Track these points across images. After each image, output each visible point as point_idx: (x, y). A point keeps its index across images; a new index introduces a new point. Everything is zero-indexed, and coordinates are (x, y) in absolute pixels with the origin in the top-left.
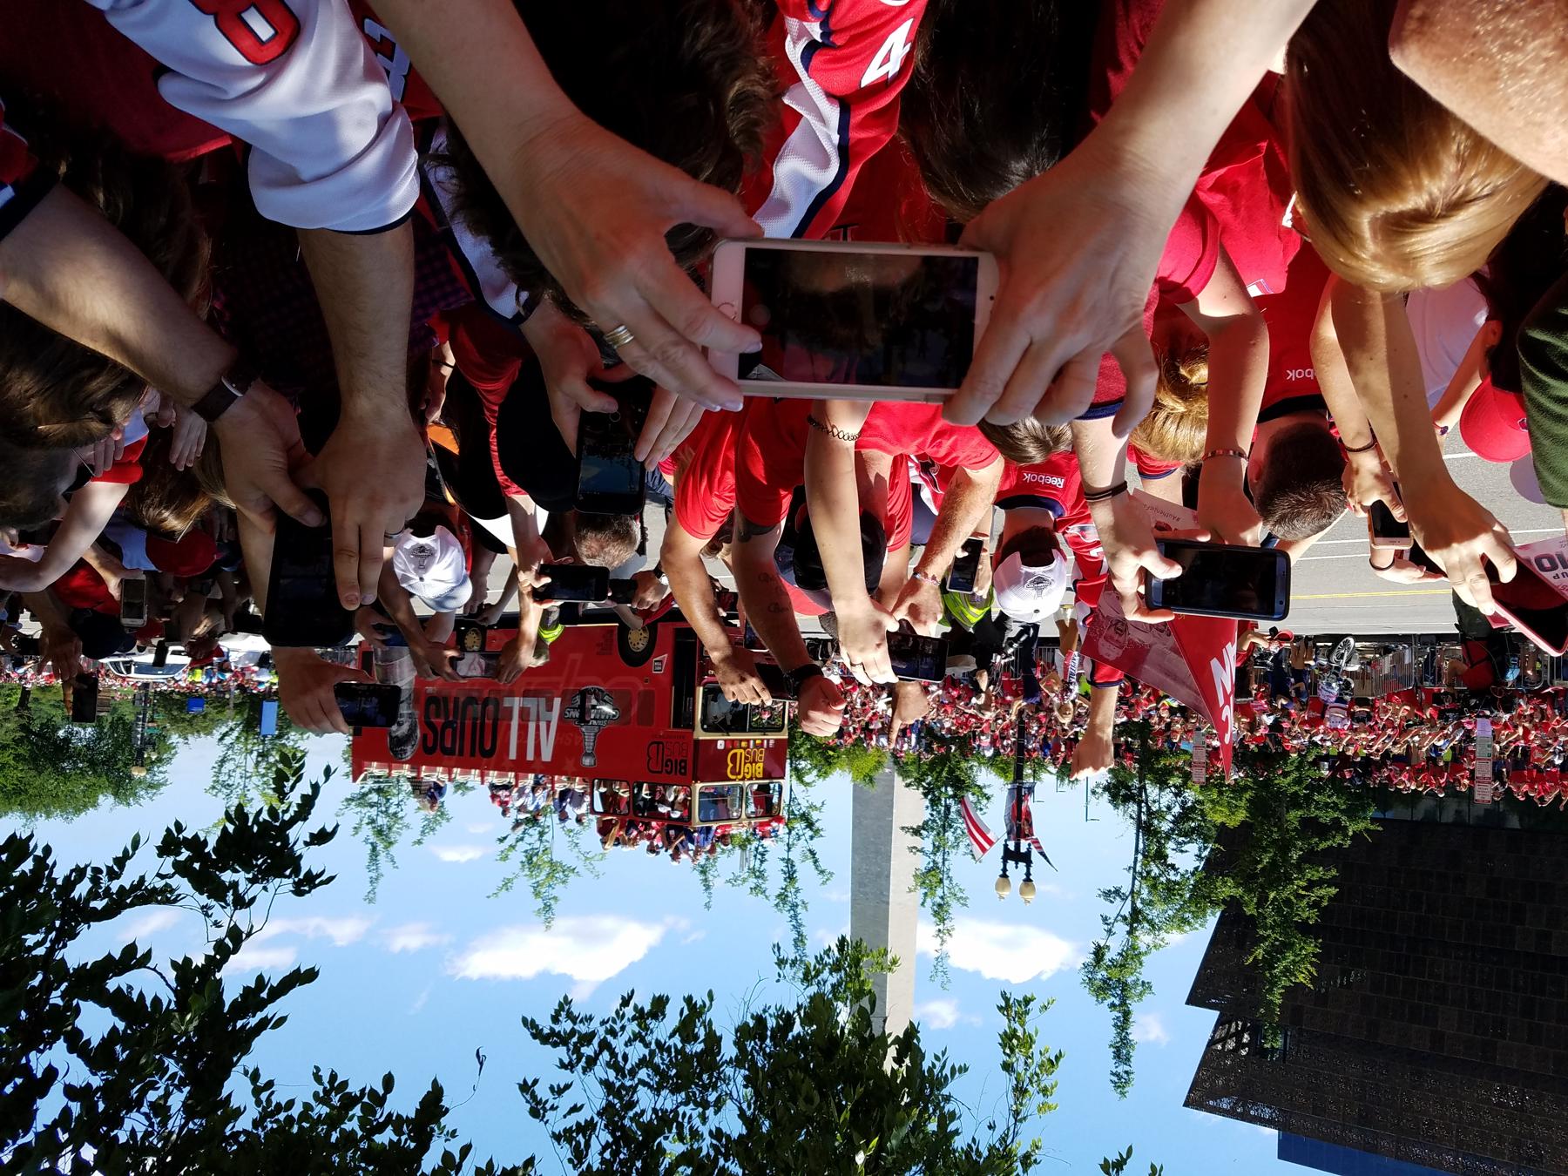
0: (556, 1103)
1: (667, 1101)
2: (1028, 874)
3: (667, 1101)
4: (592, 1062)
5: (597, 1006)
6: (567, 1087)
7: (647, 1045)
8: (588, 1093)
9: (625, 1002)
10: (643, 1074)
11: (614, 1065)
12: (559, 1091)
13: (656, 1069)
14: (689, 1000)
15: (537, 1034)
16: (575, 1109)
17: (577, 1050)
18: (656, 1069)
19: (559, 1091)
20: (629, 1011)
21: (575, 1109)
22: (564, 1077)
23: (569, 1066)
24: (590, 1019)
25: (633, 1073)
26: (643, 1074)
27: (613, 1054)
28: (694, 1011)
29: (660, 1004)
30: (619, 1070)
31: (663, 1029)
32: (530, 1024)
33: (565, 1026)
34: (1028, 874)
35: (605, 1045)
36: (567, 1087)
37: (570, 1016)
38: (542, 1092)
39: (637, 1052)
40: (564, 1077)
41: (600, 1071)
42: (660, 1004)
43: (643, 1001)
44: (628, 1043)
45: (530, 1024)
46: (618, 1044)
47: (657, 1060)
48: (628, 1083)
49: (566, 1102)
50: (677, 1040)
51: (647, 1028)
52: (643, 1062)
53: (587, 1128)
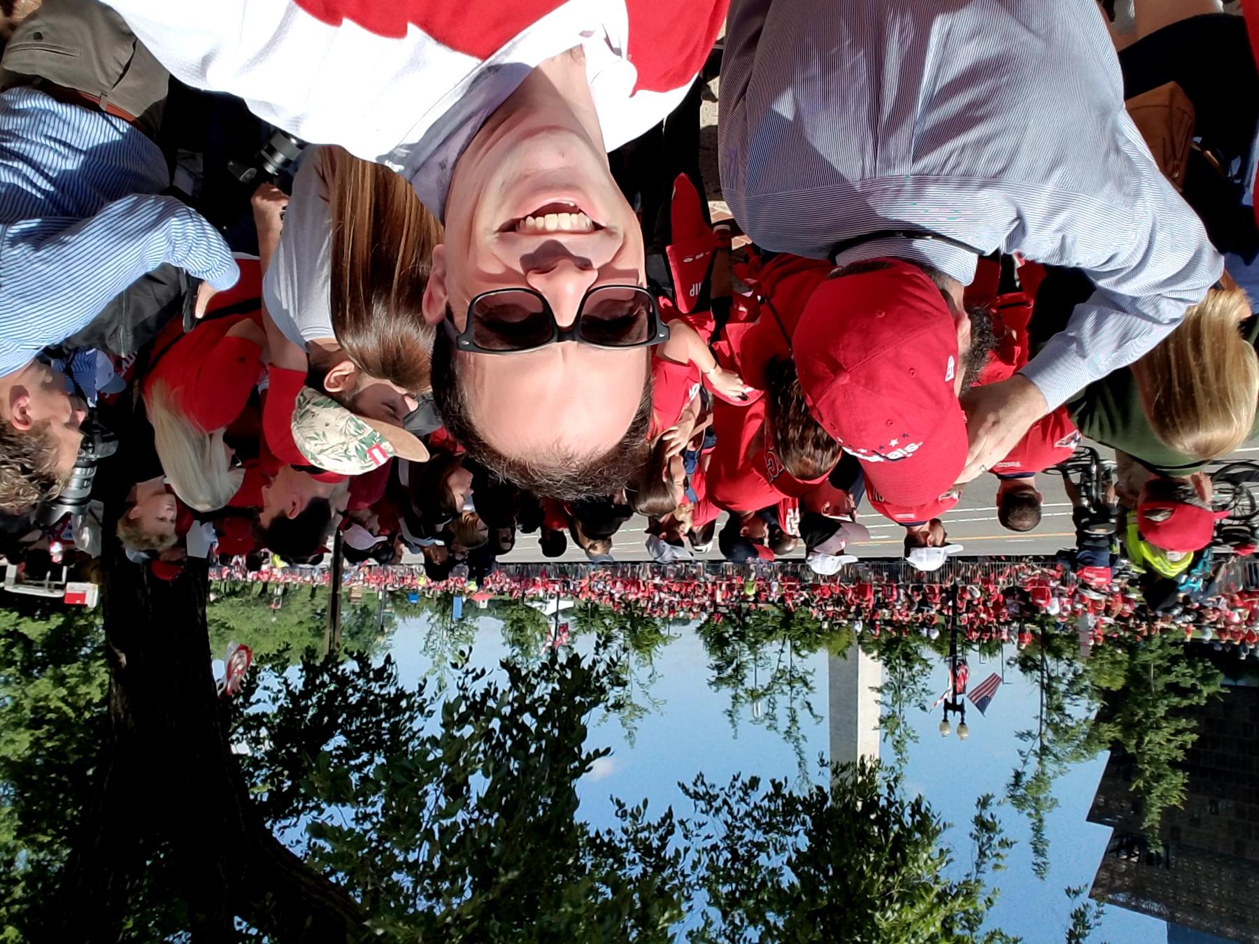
0: (700, 832)
1: (760, 837)
2: (963, 719)
3: (760, 837)
4: (718, 810)
5: (719, 780)
6: (704, 824)
7: (748, 804)
8: (716, 828)
9: (735, 779)
10: (746, 821)
11: (730, 812)
12: (700, 826)
13: (754, 819)
14: (773, 782)
15: (686, 791)
16: (708, 837)
17: (709, 803)
18: (754, 819)
19: (700, 826)
20: (738, 784)
21: (708, 837)
22: (703, 818)
23: (707, 812)
24: (713, 786)
25: (742, 820)
26: (746, 821)
27: (730, 808)
28: (777, 787)
29: (754, 782)
30: (734, 817)
31: (756, 797)
32: (683, 787)
33: (701, 790)
34: (963, 719)
35: (725, 802)
36: (704, 824)
37: (703, 783)
38: (690, 826)
39: (744, 808)
40: (703, 818)
41: (724, 814)
42: (754, 782)
43: (746, 778)
44: (737, 802)
45: (683, 787)
46: (732, 801)
47: (755, 813)
48: (738, 824)
49: (704, 832)
50: (766, 803)
51: (746, 793)
52: (748, 814)
53: (715, 847)
